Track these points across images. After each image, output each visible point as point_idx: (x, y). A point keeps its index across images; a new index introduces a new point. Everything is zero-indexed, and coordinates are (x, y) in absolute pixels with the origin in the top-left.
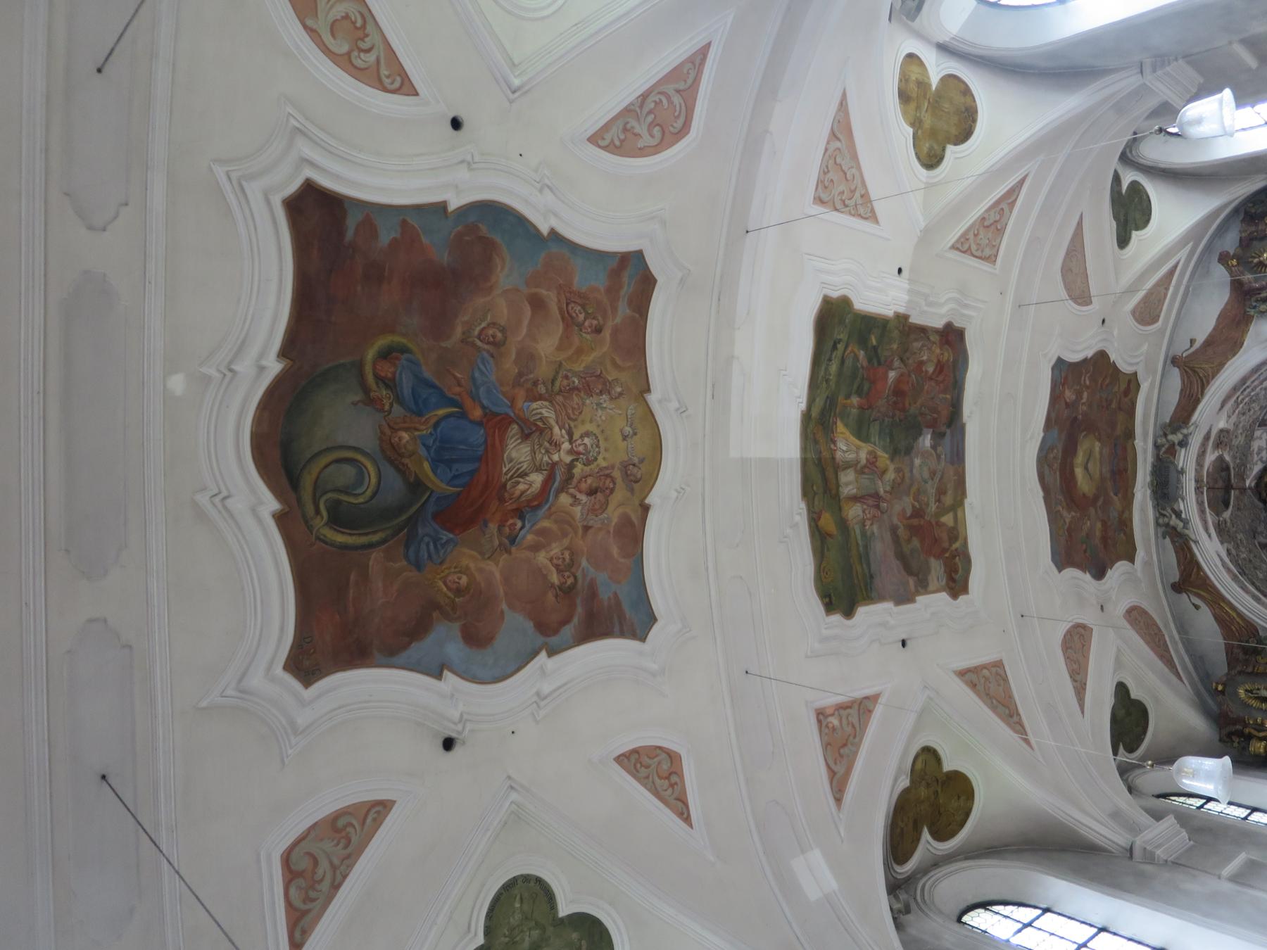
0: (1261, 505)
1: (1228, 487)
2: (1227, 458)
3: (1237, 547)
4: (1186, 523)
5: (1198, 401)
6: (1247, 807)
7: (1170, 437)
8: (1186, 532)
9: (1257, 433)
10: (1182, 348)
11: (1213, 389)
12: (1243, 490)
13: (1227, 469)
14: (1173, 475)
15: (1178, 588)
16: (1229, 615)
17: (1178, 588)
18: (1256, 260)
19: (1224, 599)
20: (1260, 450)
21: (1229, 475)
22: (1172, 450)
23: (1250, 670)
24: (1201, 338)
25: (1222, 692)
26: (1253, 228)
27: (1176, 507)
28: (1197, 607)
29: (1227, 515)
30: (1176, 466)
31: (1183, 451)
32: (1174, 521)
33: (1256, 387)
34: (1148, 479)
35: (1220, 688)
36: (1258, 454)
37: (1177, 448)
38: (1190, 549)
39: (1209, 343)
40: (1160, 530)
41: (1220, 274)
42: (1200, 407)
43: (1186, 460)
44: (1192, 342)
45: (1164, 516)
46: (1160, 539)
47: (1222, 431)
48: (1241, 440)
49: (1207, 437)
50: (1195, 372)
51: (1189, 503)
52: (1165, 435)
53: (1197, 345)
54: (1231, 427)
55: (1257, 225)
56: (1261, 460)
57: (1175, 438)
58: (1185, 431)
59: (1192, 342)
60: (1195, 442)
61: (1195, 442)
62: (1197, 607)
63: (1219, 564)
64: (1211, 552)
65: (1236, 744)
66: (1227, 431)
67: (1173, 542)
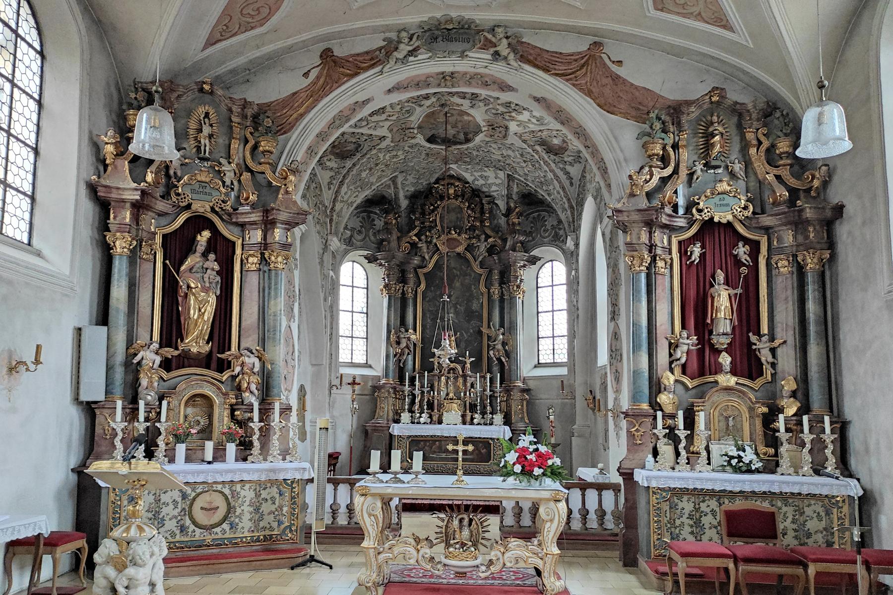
0: (433, 180)
1: (448, 142)
2: (478, 139)
3: (388, 150)
4: (404, 61)
5: (546, 70)
6: (40, 95)
7: (505, 41)
8: (392, 62)
9: (501, 174)
10: (612, 50)
11: (561, 86)
12: (446, 161)
13: (467, 140)
14: (459, 46)
15: (327, 54)
16: (300, 106)
17: (327, 54)
18: (715, 118)
19: (317, 101)
20: (486, 178)
21: (461, 143)
22: (488, 45)
23: (234, 119)
24: (621, 71)
25: (201, 90)
26: (754, 116)
27: (422, 50)
28: (306, 75)
29: (420, 140)
30: (470, 50)
31: (489, 57)
32: (404, 49)
33: (548, 165)
34: (454, 14)
35: (207, 87)
36: (481, 176)
37: (492, 50)
38: (372, 66)
39: (616, 78)
40: (393, 35)
41: (698, 90)
42: (540, 73)
43: (476, 61)
44: (620, 63)
45: (411, 39)
46: (383, 36)
47: (507, 128)
48: (496, 155)
49: (505, 87)
50: (583, 66)
51: (426, 65)
52: (507, 38)
53: (614, 68)
54: (511, 139)
55: (758, 120)
56: (476, 179)
57: (503, 48)
58: (511, 56)
59: (620, 63)
60: (498, 70)
61: (498, 70)
62: (306, 75)
63: (360, 97)
64: (373, 88)
65: (133, 95)
66: (505, 137)
67: (380, 49)
